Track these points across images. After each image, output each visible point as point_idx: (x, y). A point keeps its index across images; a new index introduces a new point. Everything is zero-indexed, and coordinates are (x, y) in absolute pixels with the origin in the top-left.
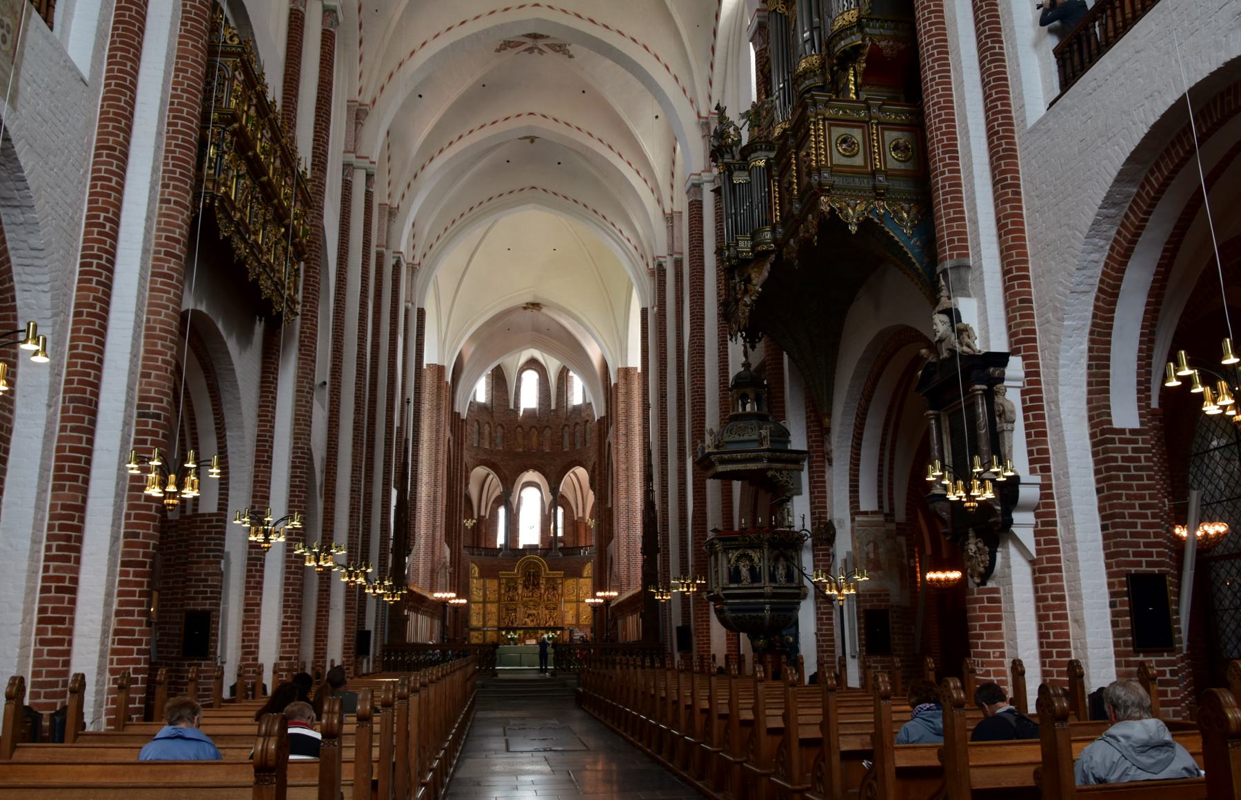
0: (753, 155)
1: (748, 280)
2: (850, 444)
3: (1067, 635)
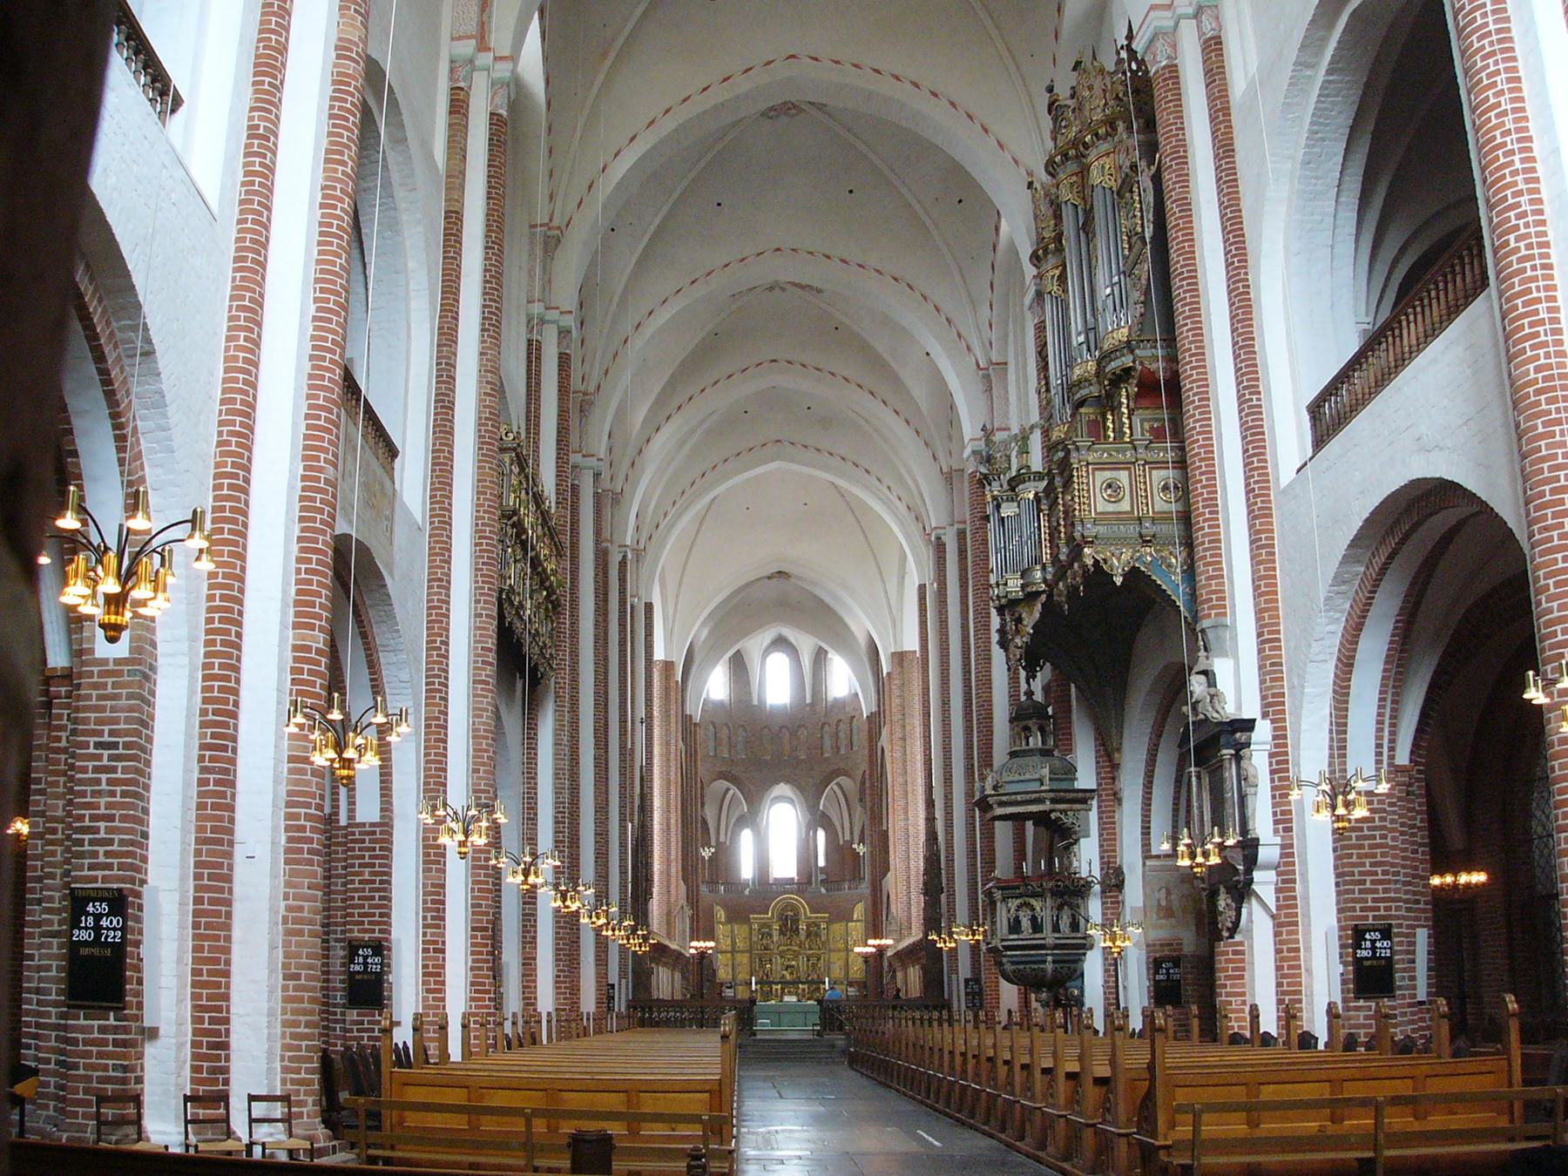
0: (1021, 487)
1: (1019, 620)
2: (1141, 781)
3: (1300, 984)
